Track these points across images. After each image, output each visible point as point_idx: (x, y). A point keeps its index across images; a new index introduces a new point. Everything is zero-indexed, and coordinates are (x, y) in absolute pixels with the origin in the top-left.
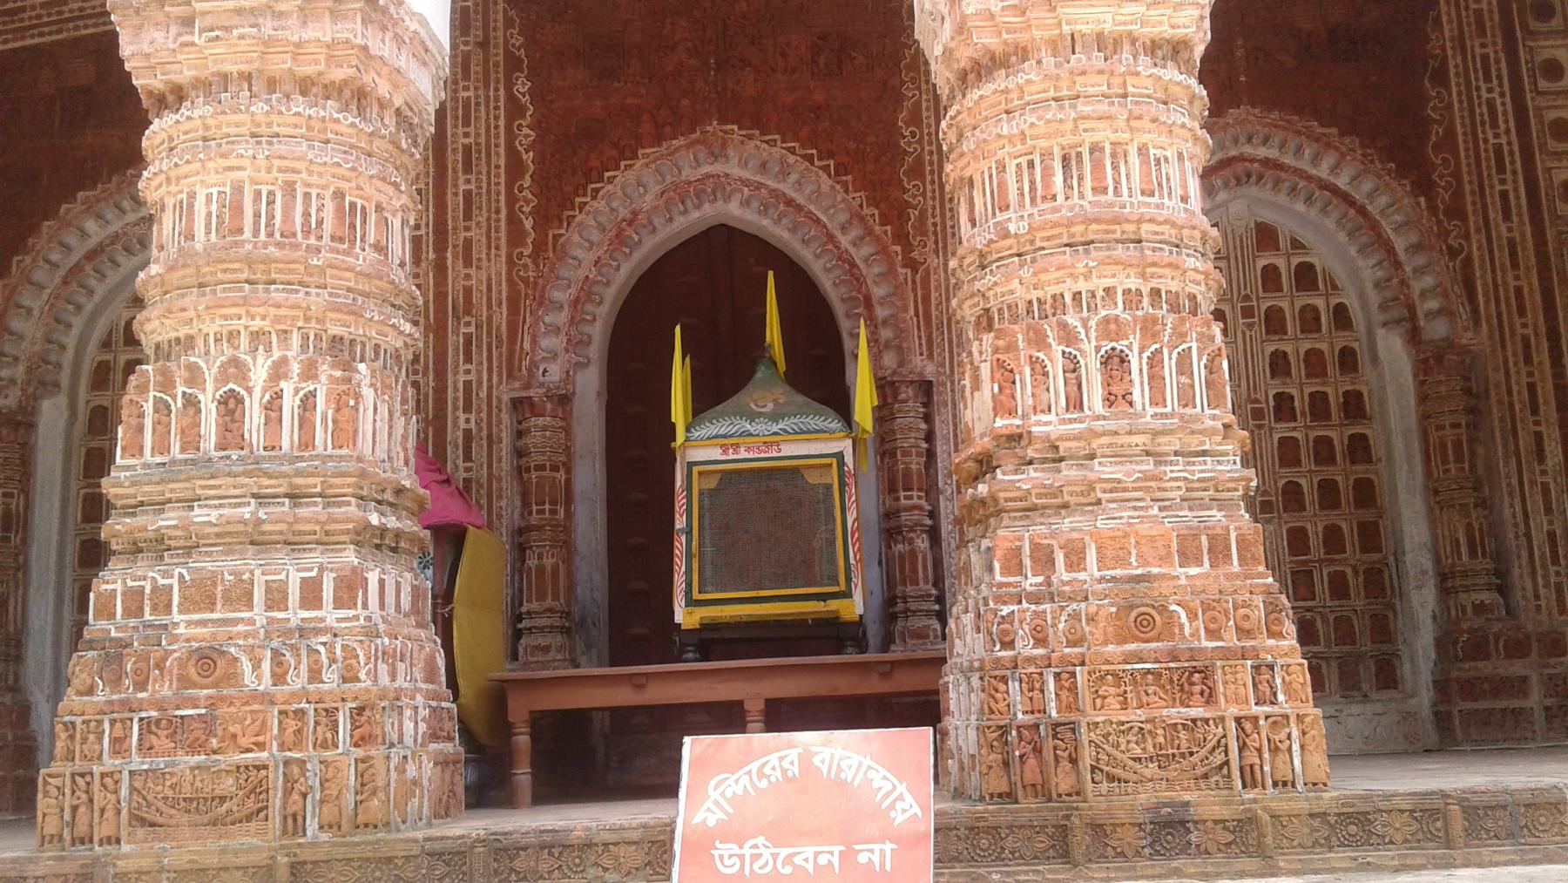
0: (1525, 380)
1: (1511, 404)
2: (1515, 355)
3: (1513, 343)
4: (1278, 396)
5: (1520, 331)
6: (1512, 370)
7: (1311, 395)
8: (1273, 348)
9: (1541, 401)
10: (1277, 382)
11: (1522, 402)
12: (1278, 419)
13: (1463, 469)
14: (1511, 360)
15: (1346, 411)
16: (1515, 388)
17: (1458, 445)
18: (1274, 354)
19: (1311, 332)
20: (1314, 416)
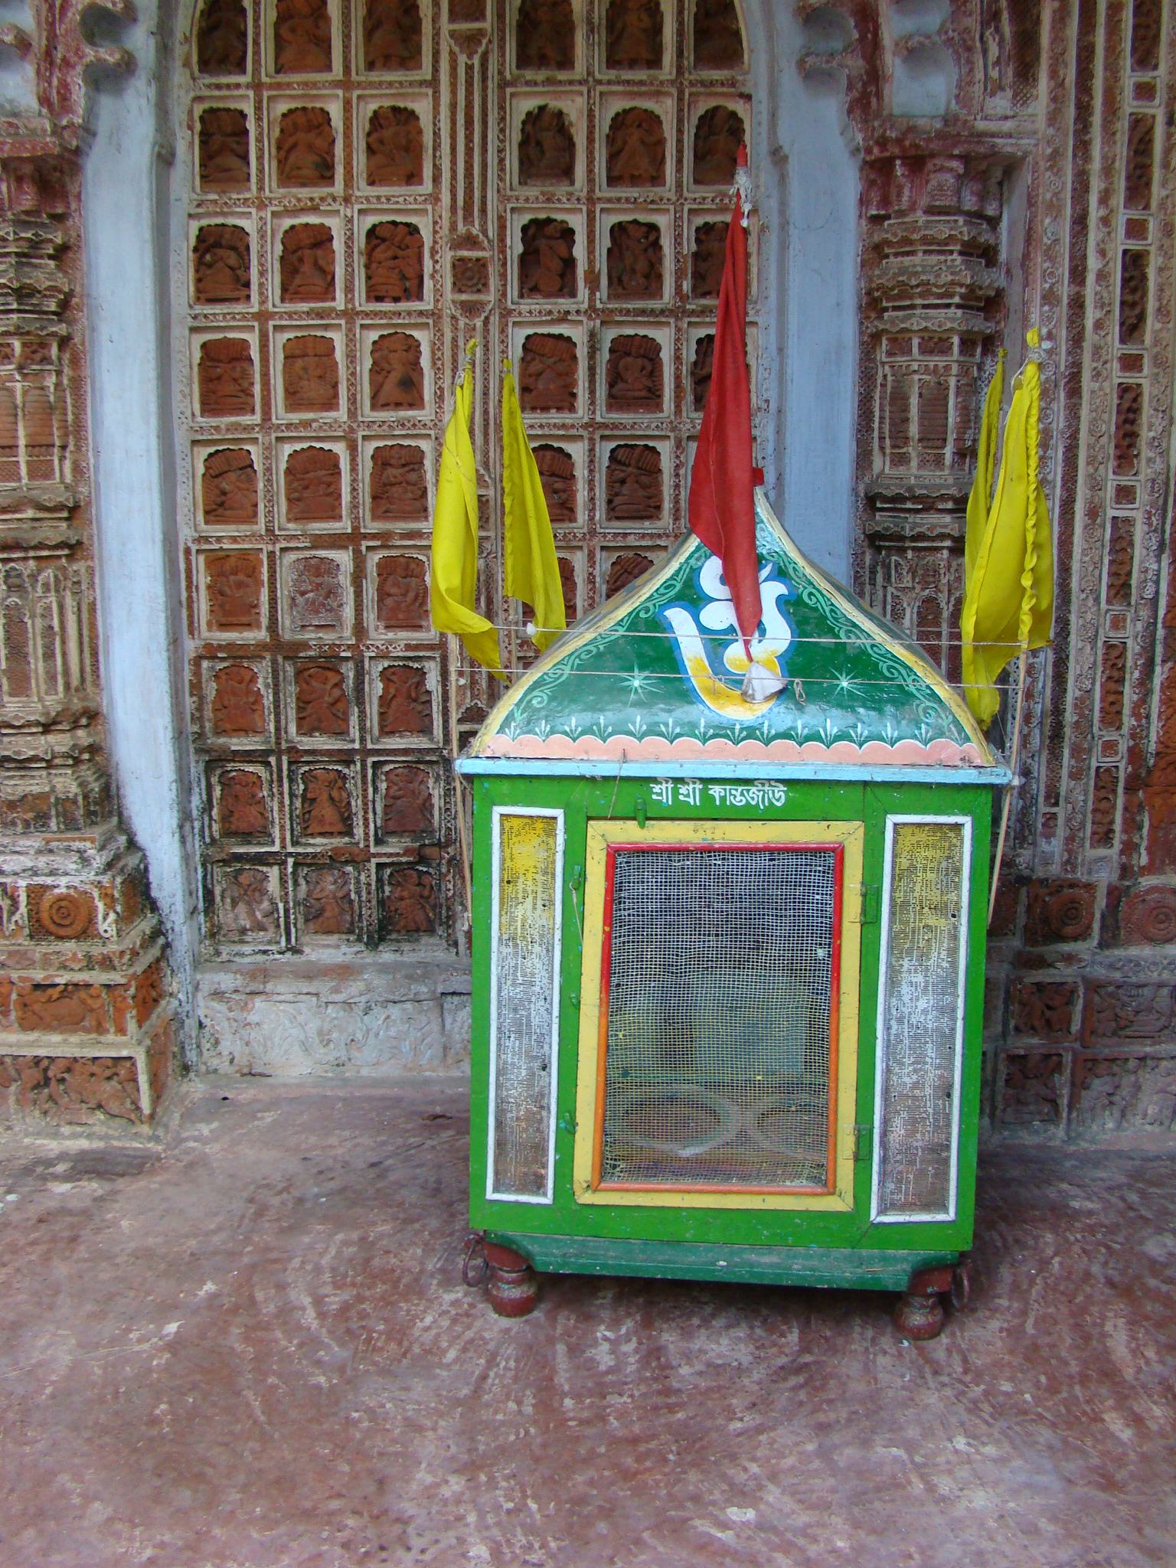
0: (1120, 242)
1: (1077, 304)
2: (1107, 171)
3: (1109, 134)
4: (534, 231)
5: (1129, 104)
6: (1095, 213)
7: (618, 230)
8: (529, 104)
9: (1151, 305)
10: (532, 191)
11: (1101, 304)
12: (529, 287)
13: (939, 461)
14: (1096, 185)
15: (698, 277)
16: (1093, 263)
17: (935, 403)
18: (533, 119)
19: (632, 64)
20: (619, 284)
